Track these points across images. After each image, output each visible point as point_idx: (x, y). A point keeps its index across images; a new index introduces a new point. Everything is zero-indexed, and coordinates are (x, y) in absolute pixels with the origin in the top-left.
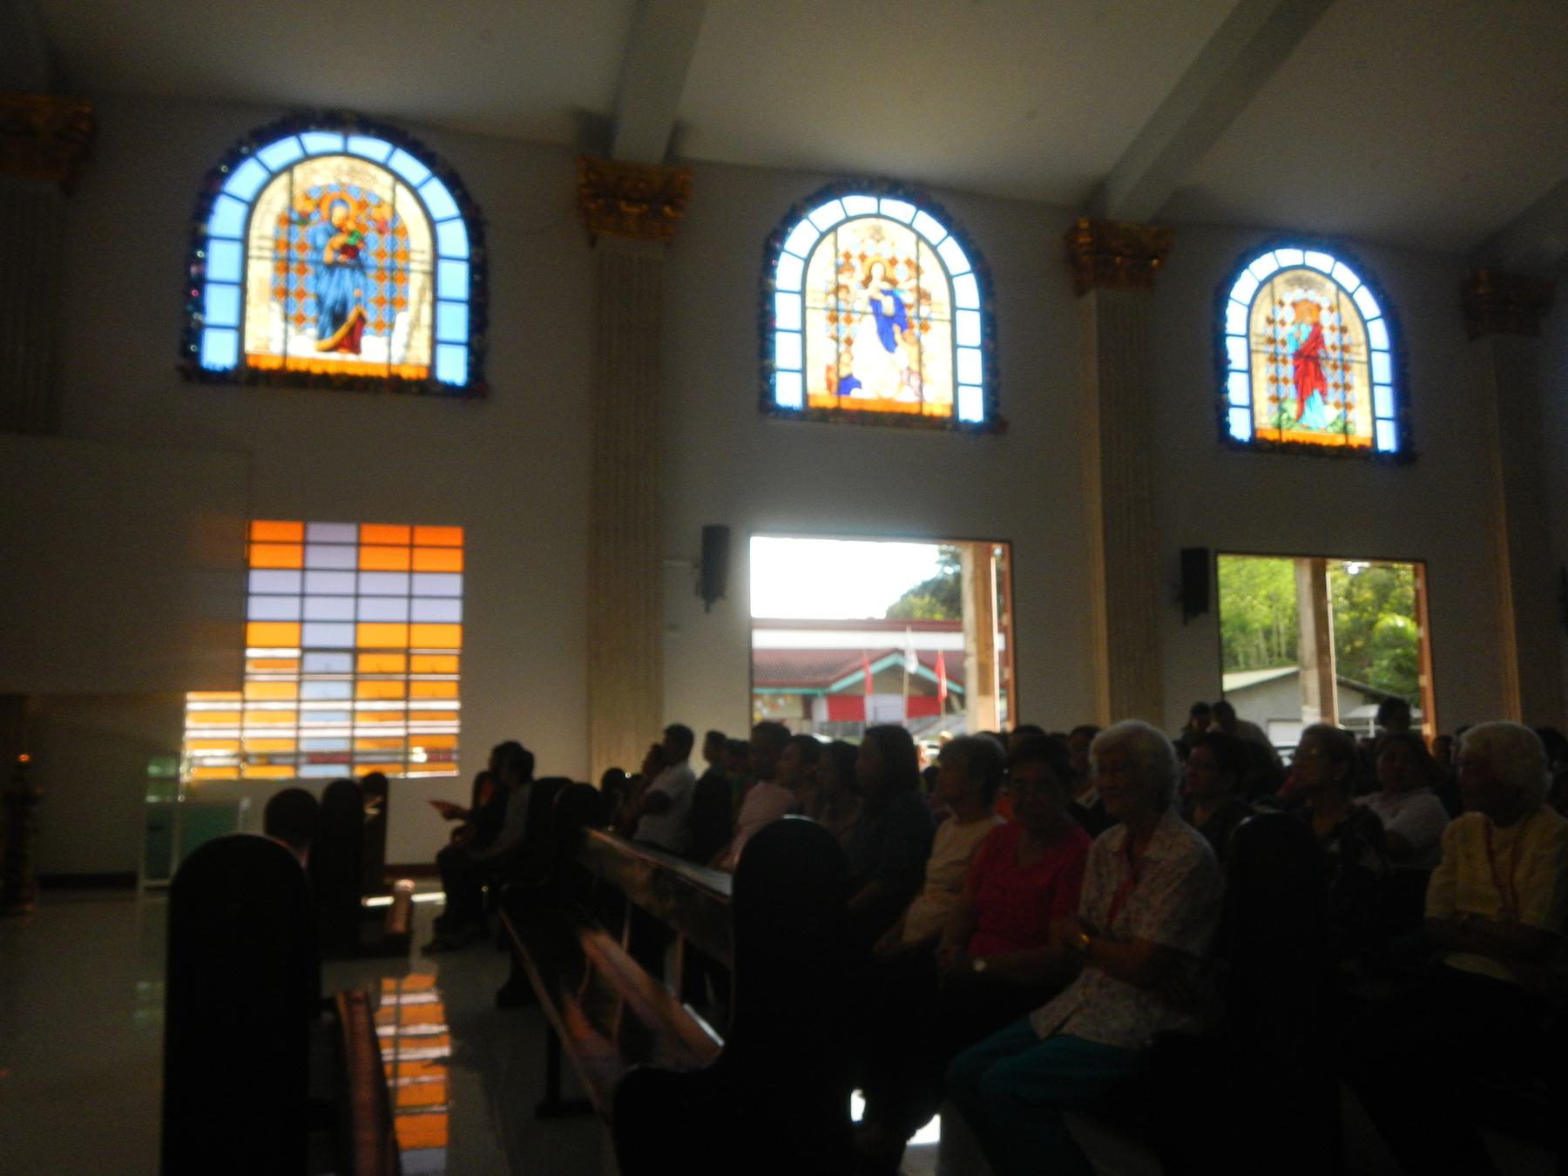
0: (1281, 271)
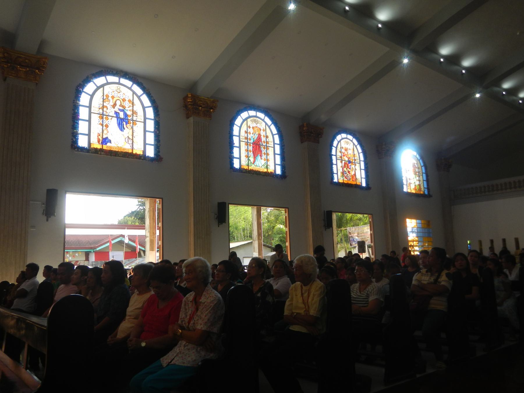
0: (250, 117)
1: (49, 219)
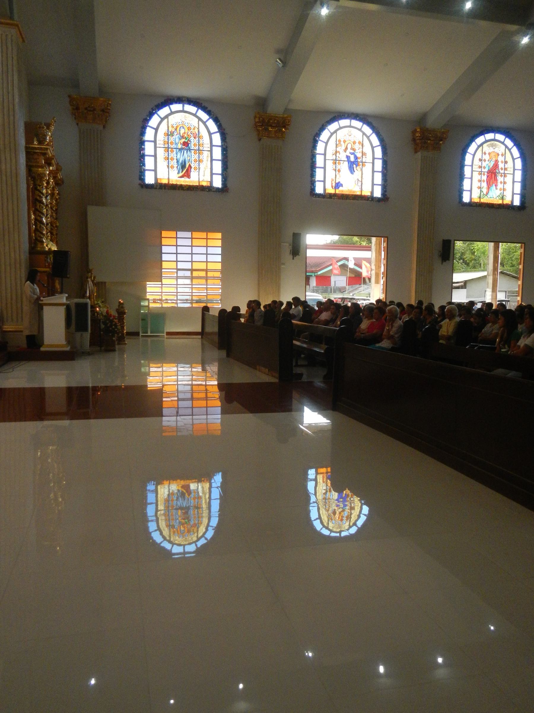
0: (486, 141)
1: (295, 258)
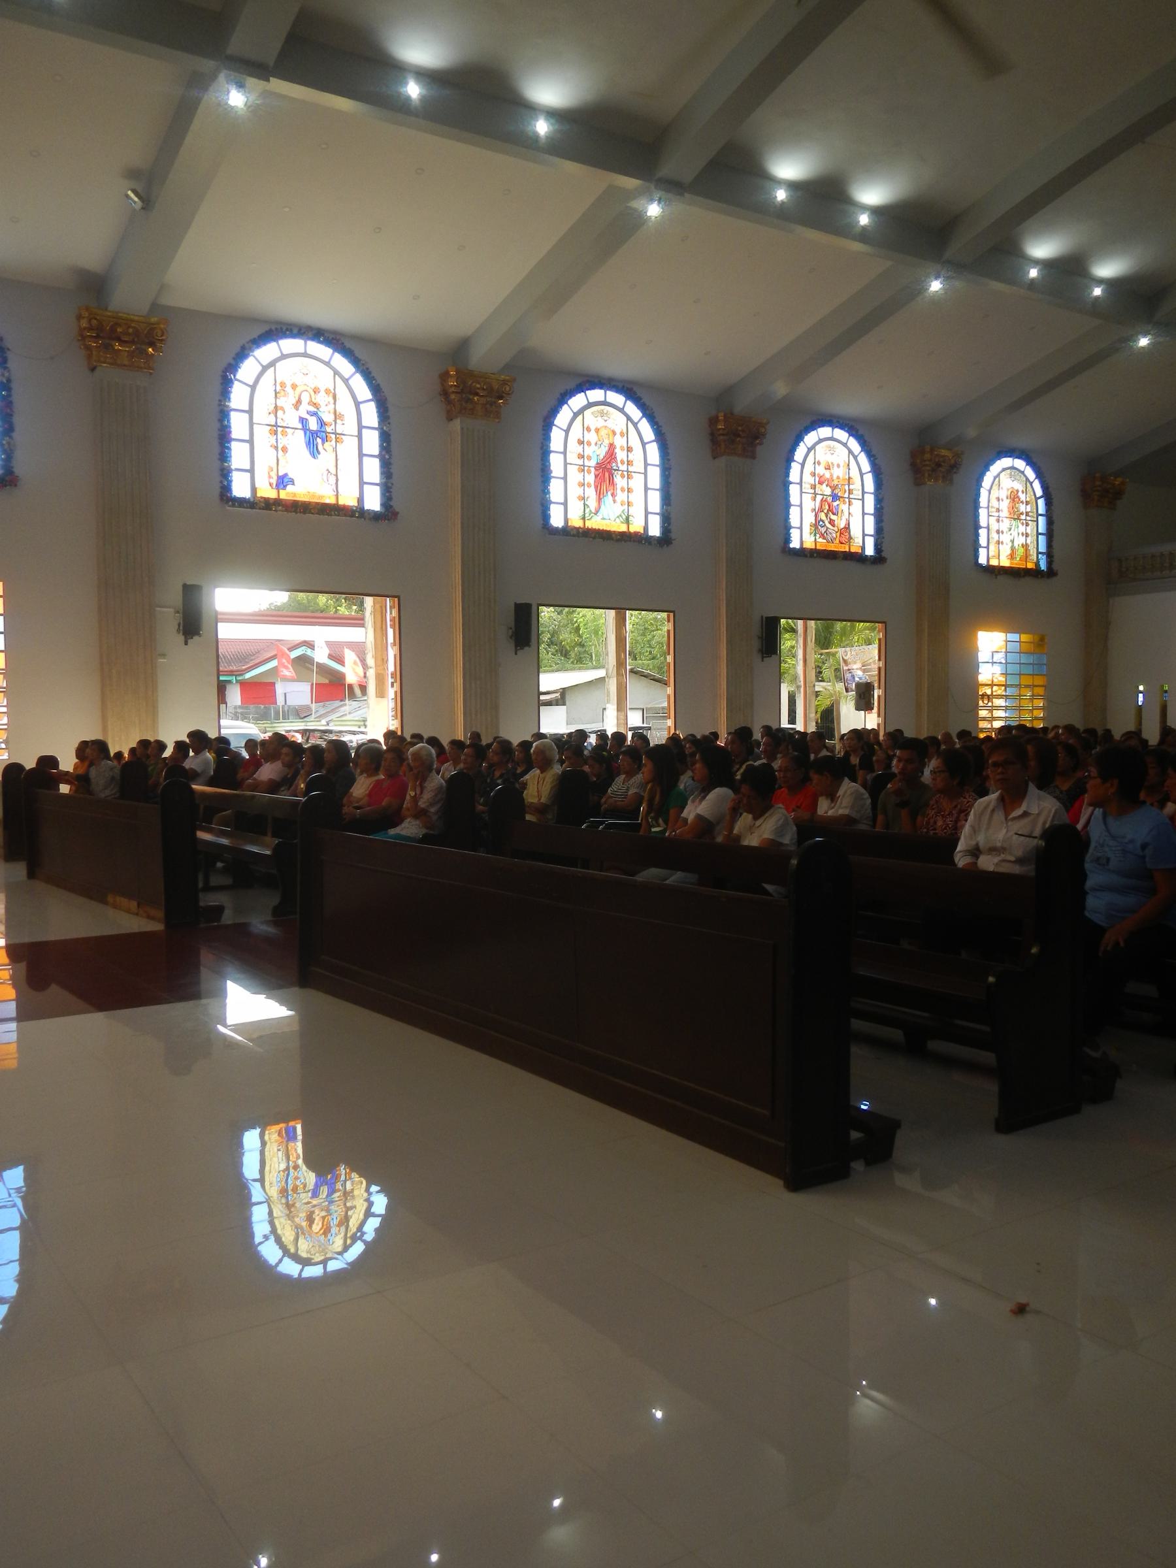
0: (590, 405)
1: (189, 641)
